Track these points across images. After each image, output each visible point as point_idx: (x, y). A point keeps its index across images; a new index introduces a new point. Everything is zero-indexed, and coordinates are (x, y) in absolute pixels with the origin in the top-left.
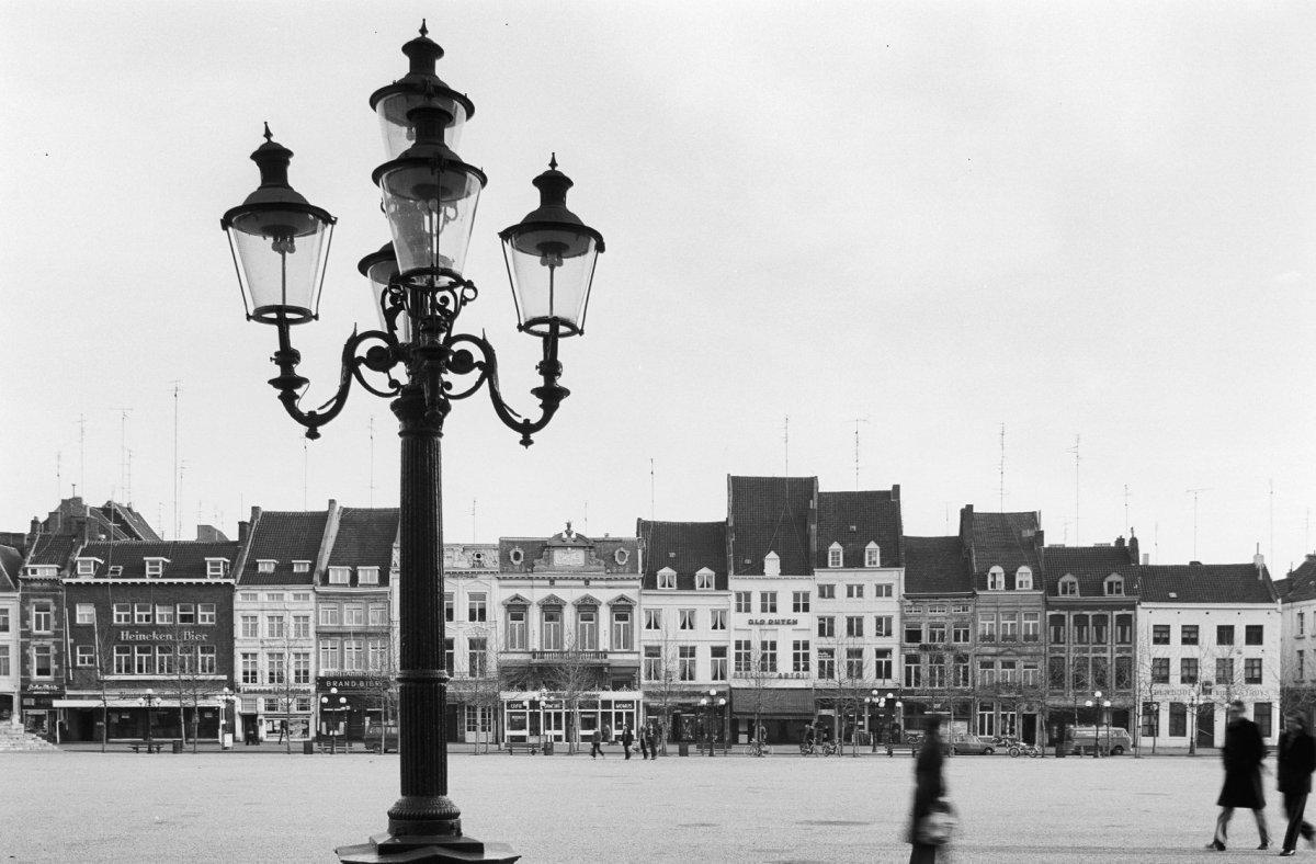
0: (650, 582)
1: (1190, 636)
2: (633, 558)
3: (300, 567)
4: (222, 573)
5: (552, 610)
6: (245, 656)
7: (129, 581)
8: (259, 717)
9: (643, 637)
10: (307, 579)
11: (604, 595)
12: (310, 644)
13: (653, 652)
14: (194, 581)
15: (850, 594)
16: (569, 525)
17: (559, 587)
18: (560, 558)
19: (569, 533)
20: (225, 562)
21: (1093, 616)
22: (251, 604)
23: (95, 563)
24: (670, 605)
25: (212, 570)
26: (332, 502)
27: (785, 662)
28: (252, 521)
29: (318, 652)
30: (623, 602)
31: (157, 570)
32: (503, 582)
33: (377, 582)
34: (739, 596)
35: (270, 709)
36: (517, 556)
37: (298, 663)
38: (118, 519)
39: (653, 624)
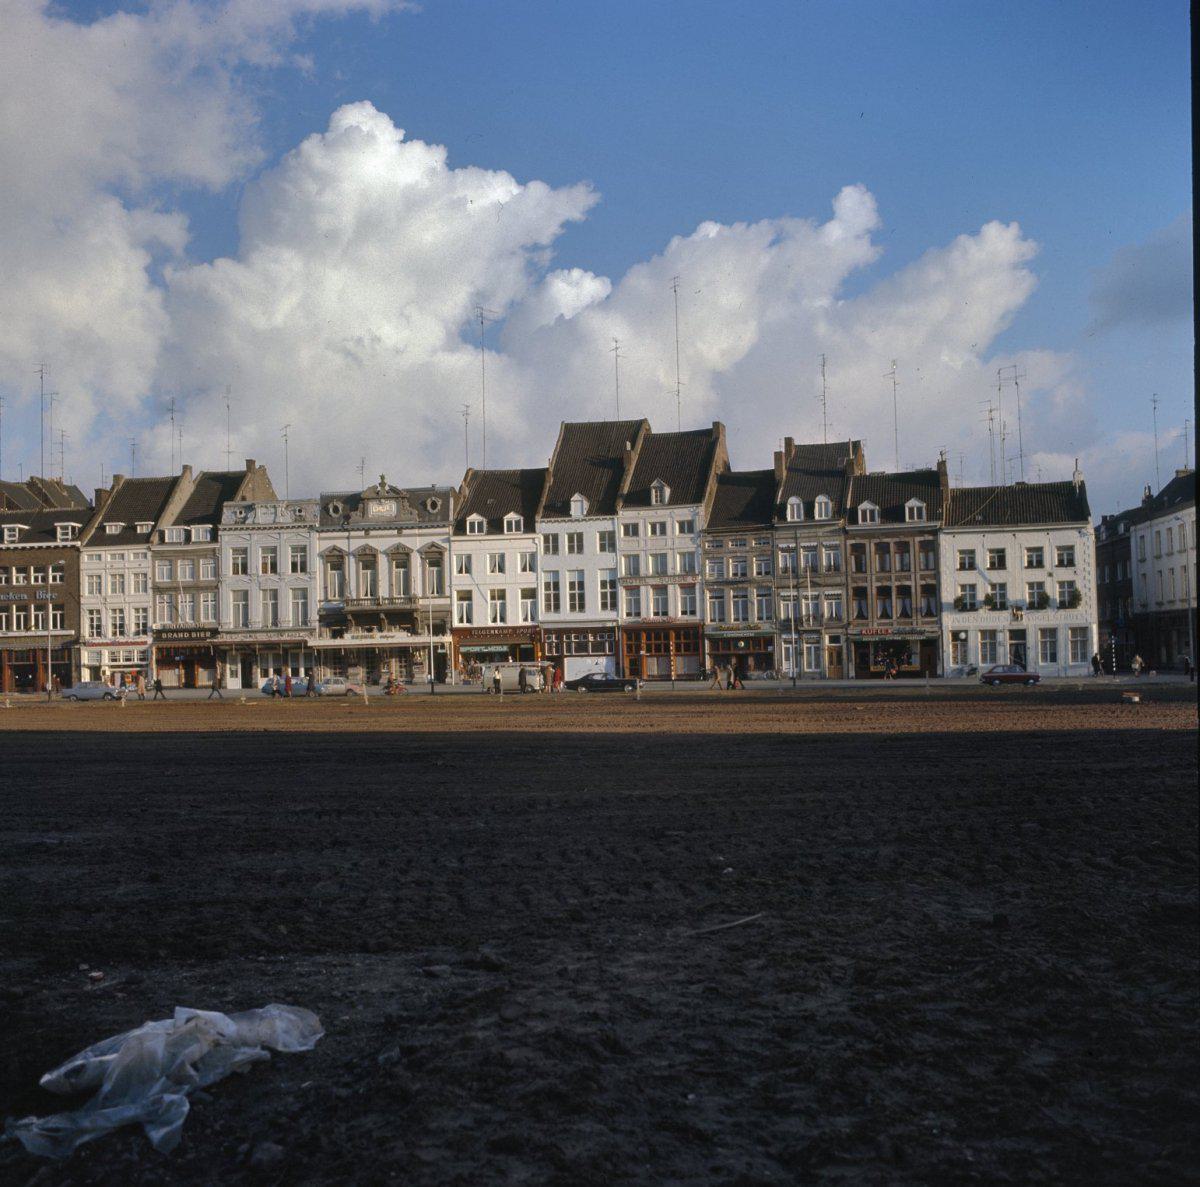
0: (460, 528)
1: (999, 560)
2: (446, 506)
3: (143, 528)
4: (70, 537)
5: (368, 559)
6: (91, 612)
7: (28, 545)
8: (103, 669)
9: (457, 581)
10: (146, 539)
11: (416, 541)
12: (147, 599)
13: (466, 596)
14: (44, 545)
15: (654, 532)
16: (382, 477)
17: (373, 537)
18: (375, 509)
19: (382, 484)
20: (73, 528)
21: (895, 543)
22: (98, 565)
23: (20, 530)
24: (480, 547)
25: (10, 536)
26: (186, 468)
27: (594, 594)
28: (113, 488)
29: (155, 606)
30: (434, 549)
31: (14, 536)
32: (323, 535)
33: (209, 539)
34: (546, 538)
35: (114, 660)
36: (336, 510)
37: (92, 620)
38: (39, 493)
39: (466, 567)
